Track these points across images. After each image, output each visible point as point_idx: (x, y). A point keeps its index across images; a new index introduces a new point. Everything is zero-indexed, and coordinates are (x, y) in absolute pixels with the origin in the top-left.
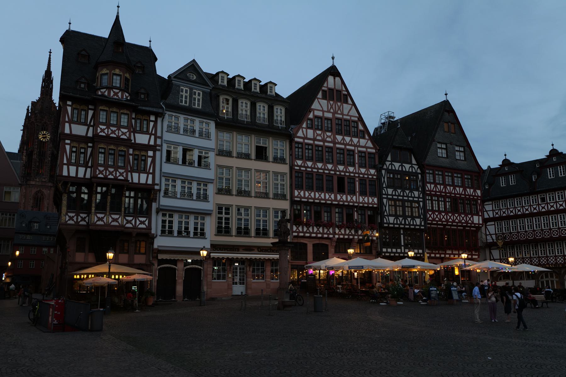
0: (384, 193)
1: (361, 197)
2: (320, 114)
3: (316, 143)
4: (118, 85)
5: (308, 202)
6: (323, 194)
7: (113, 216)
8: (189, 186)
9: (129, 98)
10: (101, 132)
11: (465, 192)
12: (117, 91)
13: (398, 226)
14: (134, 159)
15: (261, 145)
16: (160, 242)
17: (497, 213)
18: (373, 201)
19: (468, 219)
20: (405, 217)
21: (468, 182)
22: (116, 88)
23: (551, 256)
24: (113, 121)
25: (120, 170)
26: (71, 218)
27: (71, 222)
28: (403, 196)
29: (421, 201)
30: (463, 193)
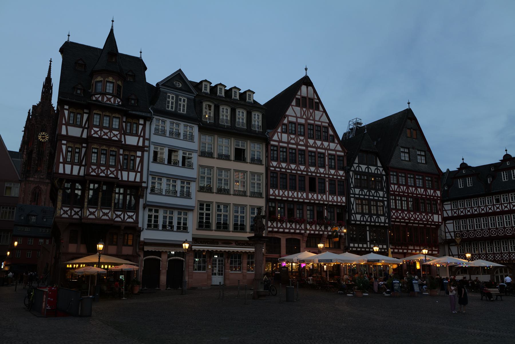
0: (352, 192)
1: (330, 196)
3: (290, 146)
4: (111, 92)
5: (282, 200)
6: (296, 193)
7: (104, 211)
8: (174, 184)
9: (120, 103)
10: (94, 134)
11: (426, 193)
12: (109, 97)
13: (364, 223)
14: (124, 159)
15: (240, 147)
16: (146, 235)
17: (455, 213)
18: (341, 199)
19: (429, 217)
20: (371, 215)
21: (429, 184)
22: (109, 94)
23: (505, 253)
24: (106, 124)
25: (111, 169)
26: (65, 212)
27: (65, 216)
28: (369, 196)
29: (385, 201)
30: (424, 193)
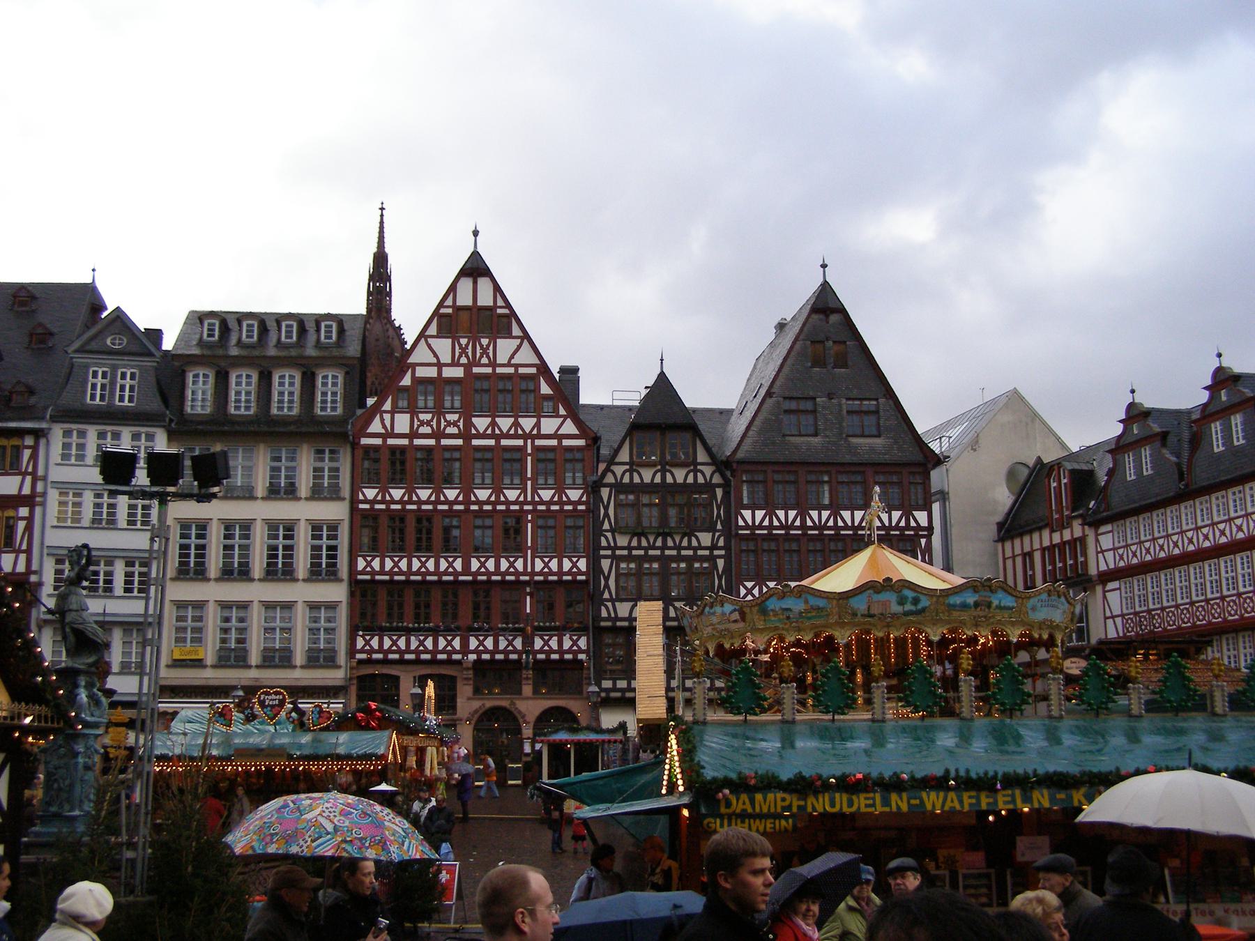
0: (604, 543)
1: (538, 561)
2: (432, 372)
3: (417, 442)
18: (574, 565)
29: (720, 557)
